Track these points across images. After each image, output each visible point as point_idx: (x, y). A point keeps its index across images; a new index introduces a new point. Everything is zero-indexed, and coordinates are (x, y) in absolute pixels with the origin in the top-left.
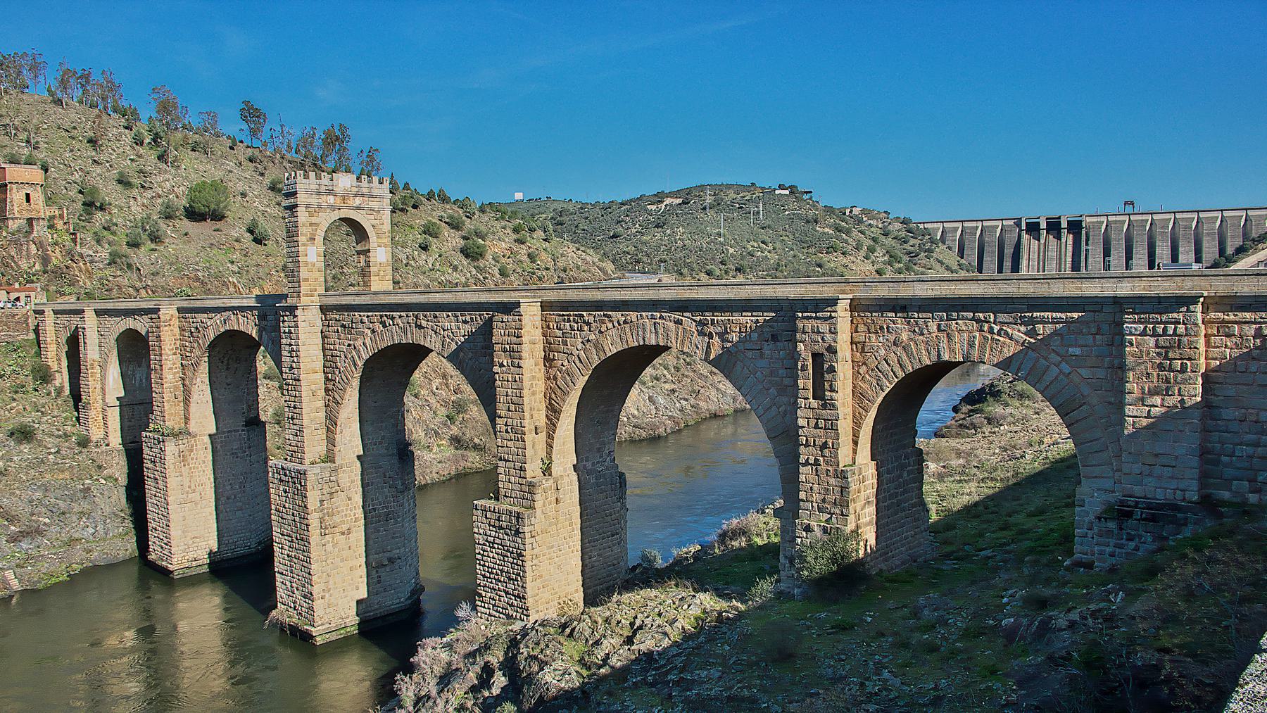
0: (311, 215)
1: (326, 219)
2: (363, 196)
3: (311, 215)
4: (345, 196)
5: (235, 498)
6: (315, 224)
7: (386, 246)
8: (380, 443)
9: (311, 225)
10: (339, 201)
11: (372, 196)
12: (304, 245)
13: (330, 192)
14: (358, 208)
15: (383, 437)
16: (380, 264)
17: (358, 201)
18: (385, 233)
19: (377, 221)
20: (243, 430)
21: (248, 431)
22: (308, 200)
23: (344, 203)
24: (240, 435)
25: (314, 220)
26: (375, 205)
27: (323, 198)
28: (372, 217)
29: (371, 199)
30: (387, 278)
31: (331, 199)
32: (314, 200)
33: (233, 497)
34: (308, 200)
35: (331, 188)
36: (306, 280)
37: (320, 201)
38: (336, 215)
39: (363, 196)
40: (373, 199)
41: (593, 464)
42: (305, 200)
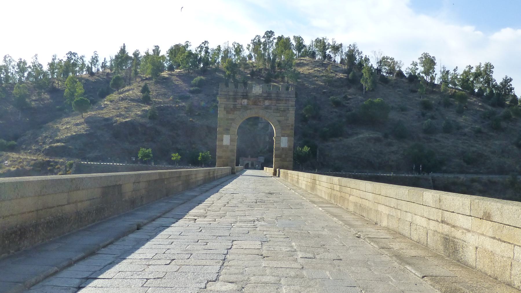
0: (228, 112)
3: (228, 112)
9: (228, 119)
13: (245, 96)
14: (267, 108)
16: (283, 149)
17: (267, 103)
18: (289, 126)
19: (283, 118)
22: (228, 103)
27: (239, 101)
28: (278, 114)
30: (288, 159)
31: (245, 102)
35: (245, 94)
39: (271, 99)
40: (280, 102)
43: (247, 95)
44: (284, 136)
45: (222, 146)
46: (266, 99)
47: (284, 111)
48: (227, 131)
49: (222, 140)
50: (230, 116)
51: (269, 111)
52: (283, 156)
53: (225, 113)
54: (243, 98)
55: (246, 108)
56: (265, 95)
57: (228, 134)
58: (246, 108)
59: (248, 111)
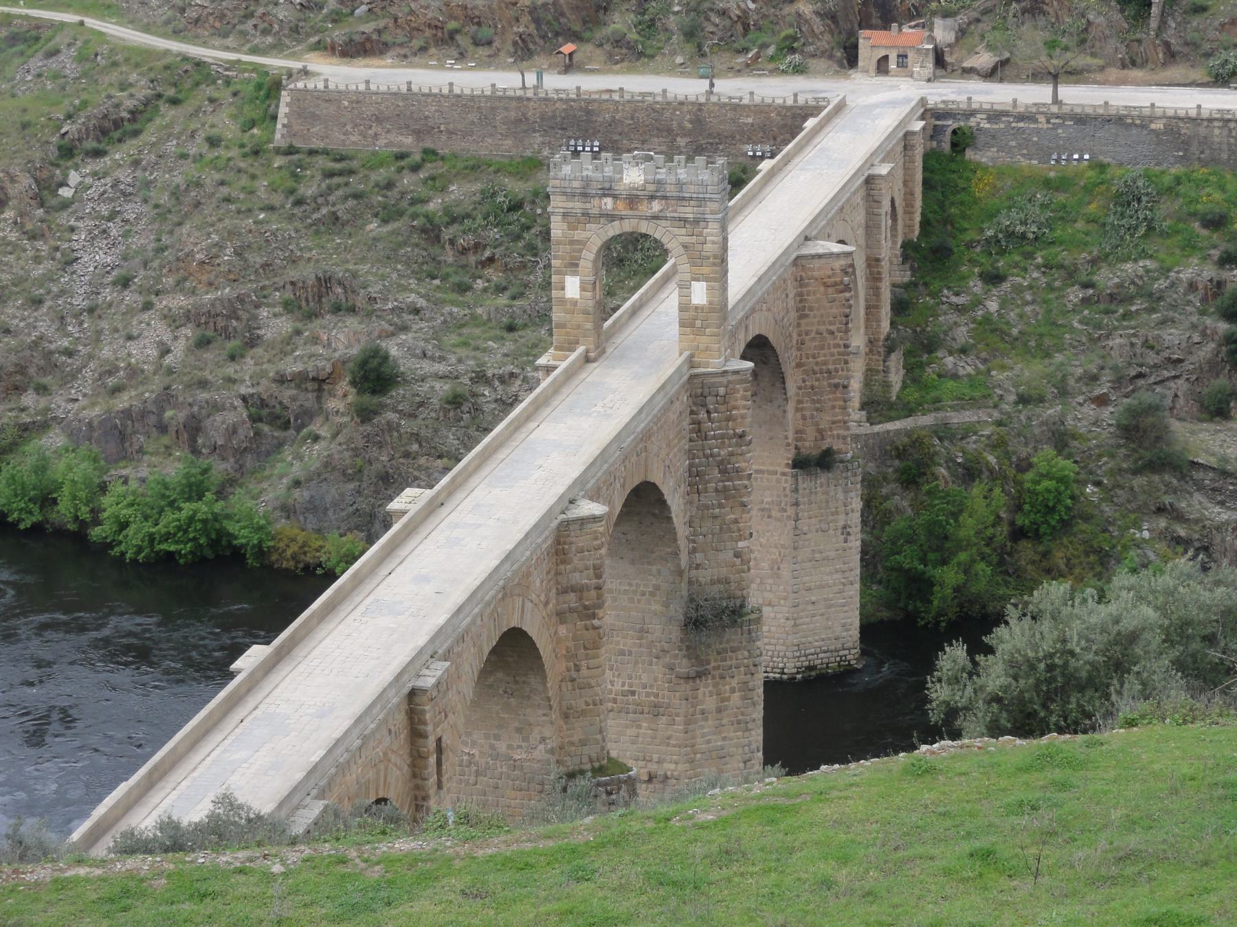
0: (572, 227)
1: (596, 236)
2: (665, 198)
3: (572, 227)
4: (633, 200)
5: (761, 583)
6: (583, 243)
7: (707, 280)
8: (652, 594)
9: (572, 242)
10: (621, 207)
11: (683, 199)
12: (558, 273)
13: (607, 192)
15: (657, 588)
16: (697, 308)
17: (656, 206)
20: (784, 474)
21: (795, 476)
22: (571, 205)
23: (631, 209)
24: (778, 481)
25: (579, 235)
26: (688, 212)
27: (596, 202)
28: (683, 231)
29: (680, 203)
31: (608, 203)
32: (577, 206)
33: (758, 581)
34: (571, 205)
35: (607, 185)
36: (561, 326)
37: (588, 206)
38: (614, 229)
39: (665, 198)
40: (684, 203)
41: (510, 747)
42: (560, 205)
43: (610, 189)
44: (697, 280)
45: (563, 301)
46: (652, 197)
47: (696, 222)
48: (573, 266)
49: (563, 289)
50: (579, 235)
51: (663, 223)
52: (698, 323)
53: (565, 226)
54: (605, 195)
55: (611, 217)
56: (651, 188)
57: (575, 273)
58: (611, 217)
59: (617, 223)
